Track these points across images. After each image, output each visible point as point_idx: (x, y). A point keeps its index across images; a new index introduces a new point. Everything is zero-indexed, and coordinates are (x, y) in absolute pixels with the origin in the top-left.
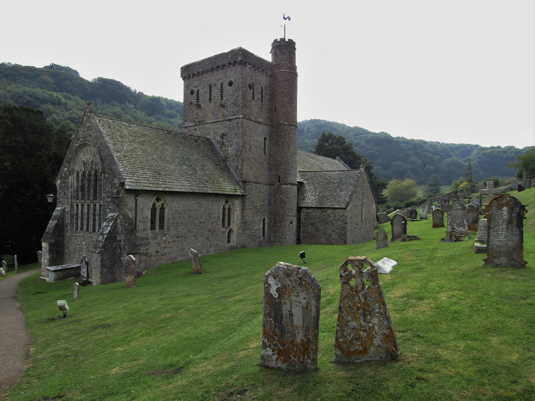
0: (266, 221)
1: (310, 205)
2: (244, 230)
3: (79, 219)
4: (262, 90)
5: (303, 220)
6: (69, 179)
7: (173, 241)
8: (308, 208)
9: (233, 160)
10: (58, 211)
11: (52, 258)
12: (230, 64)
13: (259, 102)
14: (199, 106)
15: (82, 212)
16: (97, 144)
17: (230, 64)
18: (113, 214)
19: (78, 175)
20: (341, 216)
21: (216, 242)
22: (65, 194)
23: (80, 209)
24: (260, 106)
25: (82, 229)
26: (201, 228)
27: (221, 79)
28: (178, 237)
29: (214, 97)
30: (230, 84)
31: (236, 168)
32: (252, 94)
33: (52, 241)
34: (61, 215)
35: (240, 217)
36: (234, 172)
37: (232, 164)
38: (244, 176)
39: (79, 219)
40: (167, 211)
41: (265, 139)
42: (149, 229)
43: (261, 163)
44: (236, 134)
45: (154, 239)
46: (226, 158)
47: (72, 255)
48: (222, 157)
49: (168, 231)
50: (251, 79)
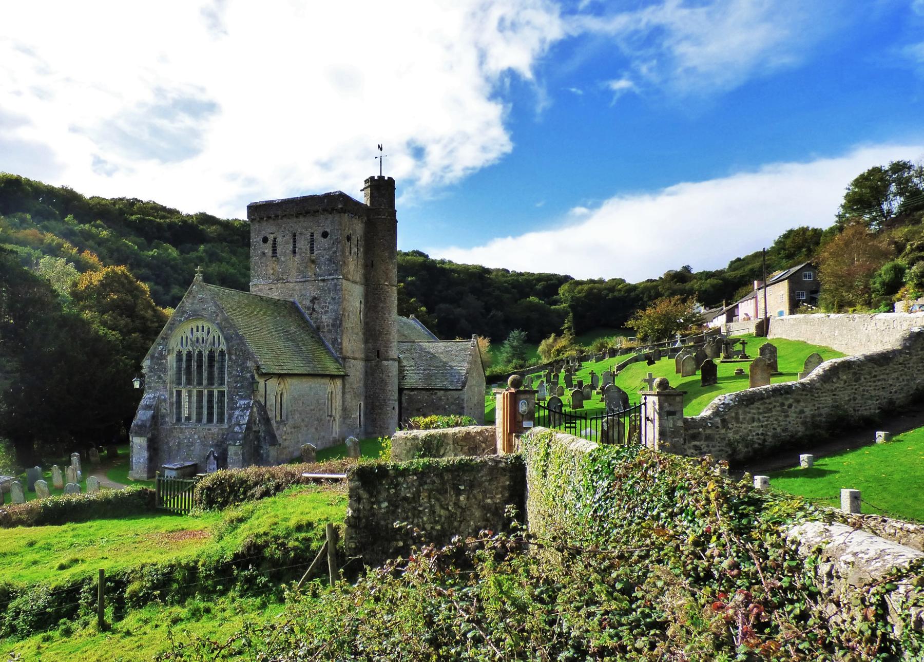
1: (415, 386)
2: (344, 418)
5: (405, 404)
8: (412, 390)
9: (330, 331)
16: (216, 319)
17: (325, 210)
20: (456, 400)
21: (322, 434)
22: (160, 377)
27: (311, 228)
30: (325, 235)
31: (334, 341)
33: (149, 435)
36: (330, 346)
37: (327, 338)
38: (344, 350)
40: (285, 396)
43: (357, 334)
44: (334, 299)
46: (318, 328)
48: (311, 326)
49: (287, 420)
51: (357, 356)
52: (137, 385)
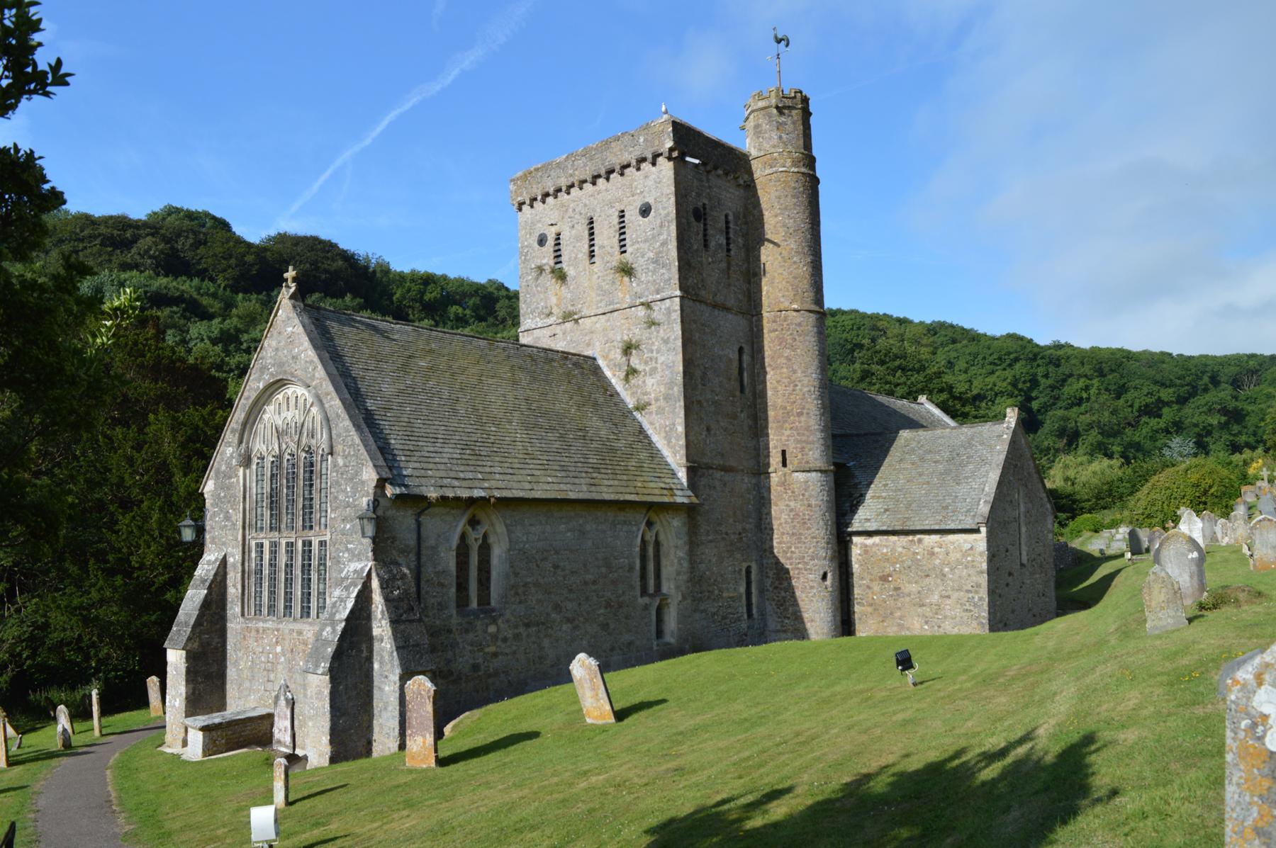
0: (753, 576)
3: (266, 584)
4: (727, 222)
6: (237, 476)
7: (517, 637)
9: (660, 411)
10: (209, 563)
11: (193, 693)
12: (642, 160)
13: (722, 254)
14: (561, 276)
15: (273, 565)
18: (358, 565)
19: (261, 466)
20: (965, 554)
21: (627, 637)
22: (227, 518)
23: (266, 556)
24: (724, 265)
25: (272, 609)
26: (587, 599)
27: (620, 201)
28: (527, 625)
29: (602, 247)
30: (645, 211)
32: (701, 236)
34: (216, 575)
35: (686, 564)
39: (266, 584)
41: (741, 350)
42: (453, 604)
44: (666, 341)
45: (467, 631)
47: (247, 684)
50: (699, 195)
51: (732, 462)
52: (188, 535)
